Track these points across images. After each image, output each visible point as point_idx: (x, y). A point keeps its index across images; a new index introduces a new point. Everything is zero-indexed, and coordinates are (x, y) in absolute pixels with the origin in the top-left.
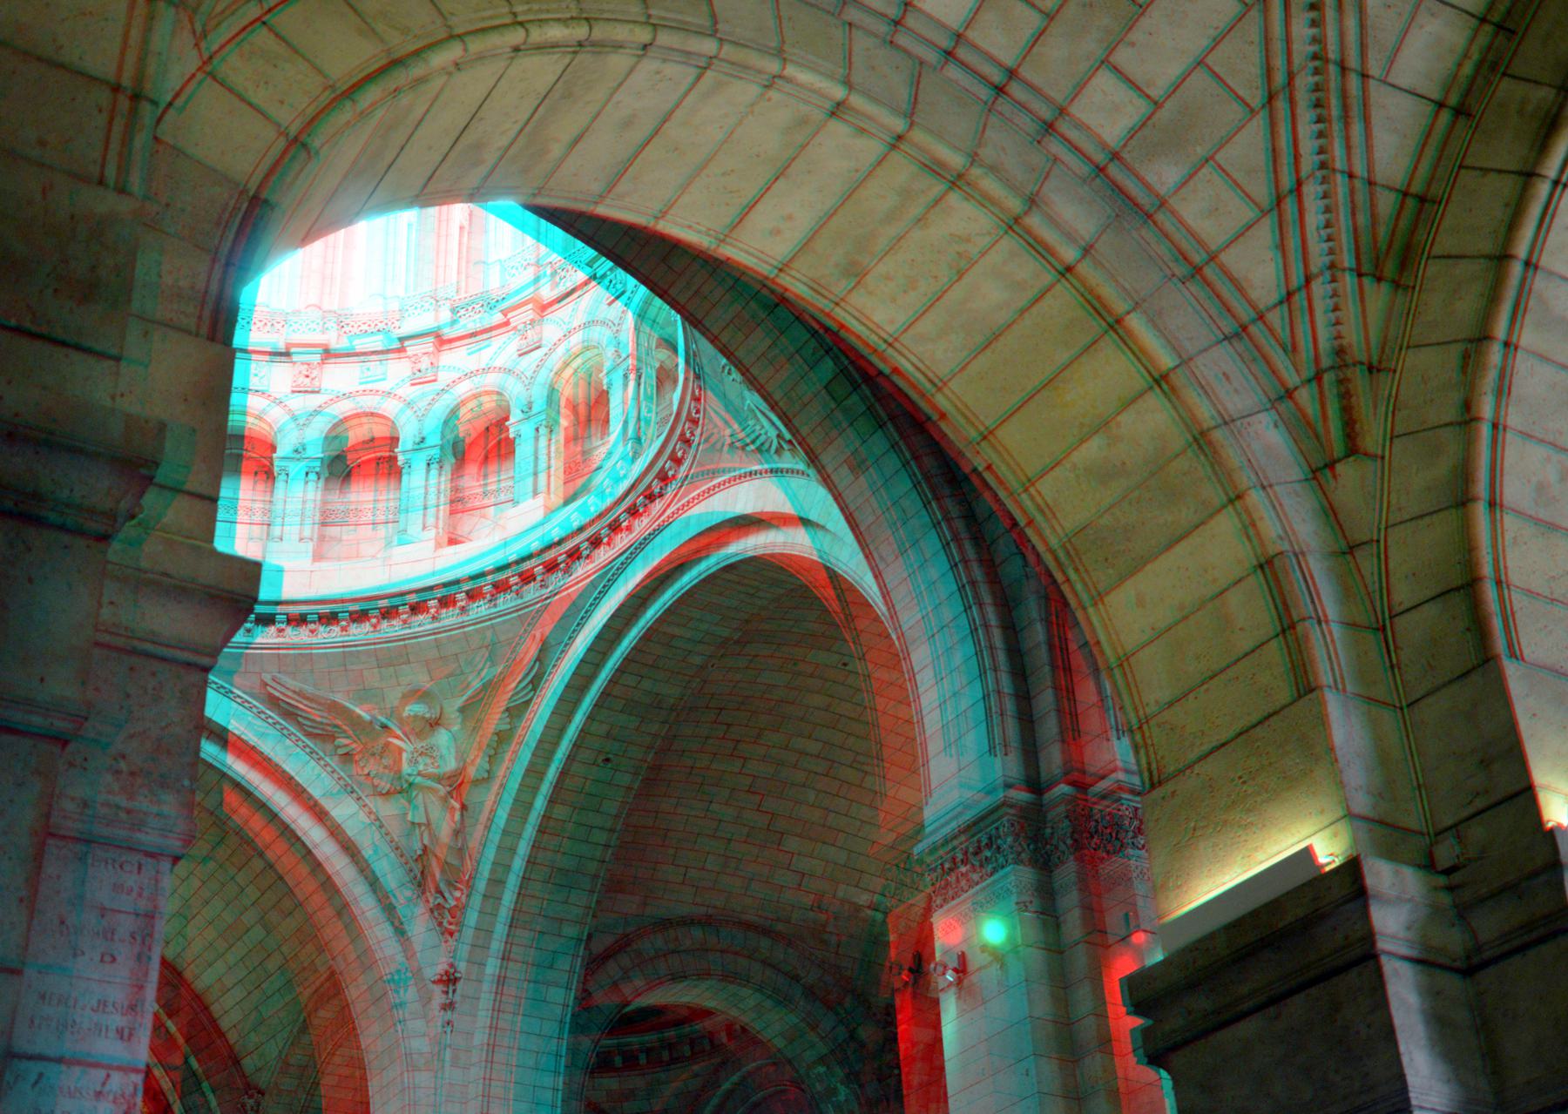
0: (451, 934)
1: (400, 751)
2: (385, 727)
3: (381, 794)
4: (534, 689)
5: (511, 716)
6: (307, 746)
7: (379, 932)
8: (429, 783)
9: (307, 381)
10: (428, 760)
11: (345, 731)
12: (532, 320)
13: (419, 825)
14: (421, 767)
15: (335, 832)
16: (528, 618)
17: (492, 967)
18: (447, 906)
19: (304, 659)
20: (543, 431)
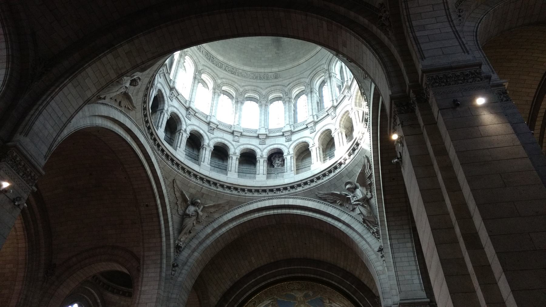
0: (379, 238)
1: (350, 198)
4: (371, 170)
5: (370, 179)
6: (331, 206)
7: (362, 244)
8: (357, 203)
9: (312, 130)
10: (355, 197)
11: (338, 199)
12: (348, 91)
13: (360, 214)
14: (354, 200)
18: (375, 232)
19: (322, 186)
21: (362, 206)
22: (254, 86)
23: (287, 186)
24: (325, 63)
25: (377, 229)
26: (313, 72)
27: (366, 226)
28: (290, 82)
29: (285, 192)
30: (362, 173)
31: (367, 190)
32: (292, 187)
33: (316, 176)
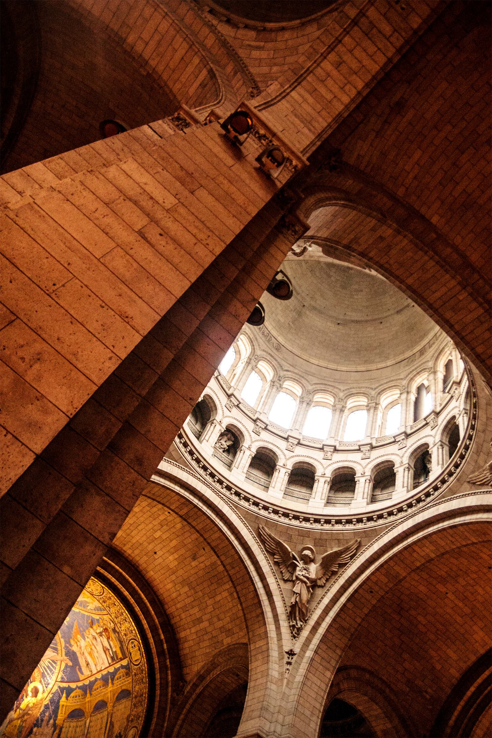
0: (295, 637)
2: (293, 555)
3: (284, 580)
4: (351, 559)
7: (271, 627)
8: (305, 579)
10: (305, 571)
13: (297, 593)
14: (303, 573)
15: (266, 587)
16: (356, 533)
17: (309, 654)
19: (274, 525)
20: (368, 481)
21: (308, 588)
22: (255, 335)
23: (233, 486)
24: (344, 391)
25: (301, 625)
26: (321, 386)
27: (288, 611)
28: (289, 369)
29: (224, 491)
30: (337, 555)
31: (324, 575)
32: (237, 494)
33: (275, 508)
